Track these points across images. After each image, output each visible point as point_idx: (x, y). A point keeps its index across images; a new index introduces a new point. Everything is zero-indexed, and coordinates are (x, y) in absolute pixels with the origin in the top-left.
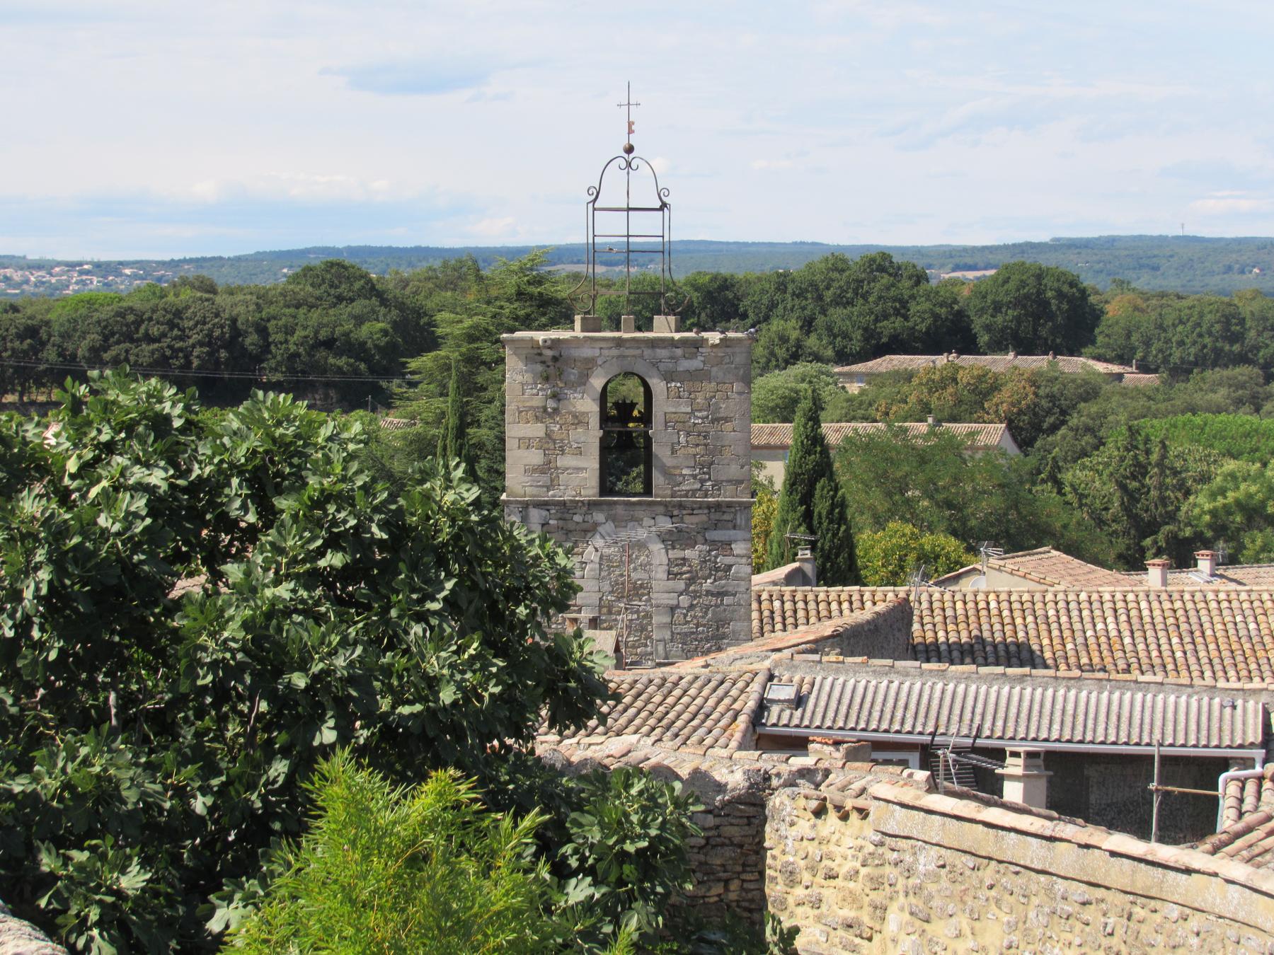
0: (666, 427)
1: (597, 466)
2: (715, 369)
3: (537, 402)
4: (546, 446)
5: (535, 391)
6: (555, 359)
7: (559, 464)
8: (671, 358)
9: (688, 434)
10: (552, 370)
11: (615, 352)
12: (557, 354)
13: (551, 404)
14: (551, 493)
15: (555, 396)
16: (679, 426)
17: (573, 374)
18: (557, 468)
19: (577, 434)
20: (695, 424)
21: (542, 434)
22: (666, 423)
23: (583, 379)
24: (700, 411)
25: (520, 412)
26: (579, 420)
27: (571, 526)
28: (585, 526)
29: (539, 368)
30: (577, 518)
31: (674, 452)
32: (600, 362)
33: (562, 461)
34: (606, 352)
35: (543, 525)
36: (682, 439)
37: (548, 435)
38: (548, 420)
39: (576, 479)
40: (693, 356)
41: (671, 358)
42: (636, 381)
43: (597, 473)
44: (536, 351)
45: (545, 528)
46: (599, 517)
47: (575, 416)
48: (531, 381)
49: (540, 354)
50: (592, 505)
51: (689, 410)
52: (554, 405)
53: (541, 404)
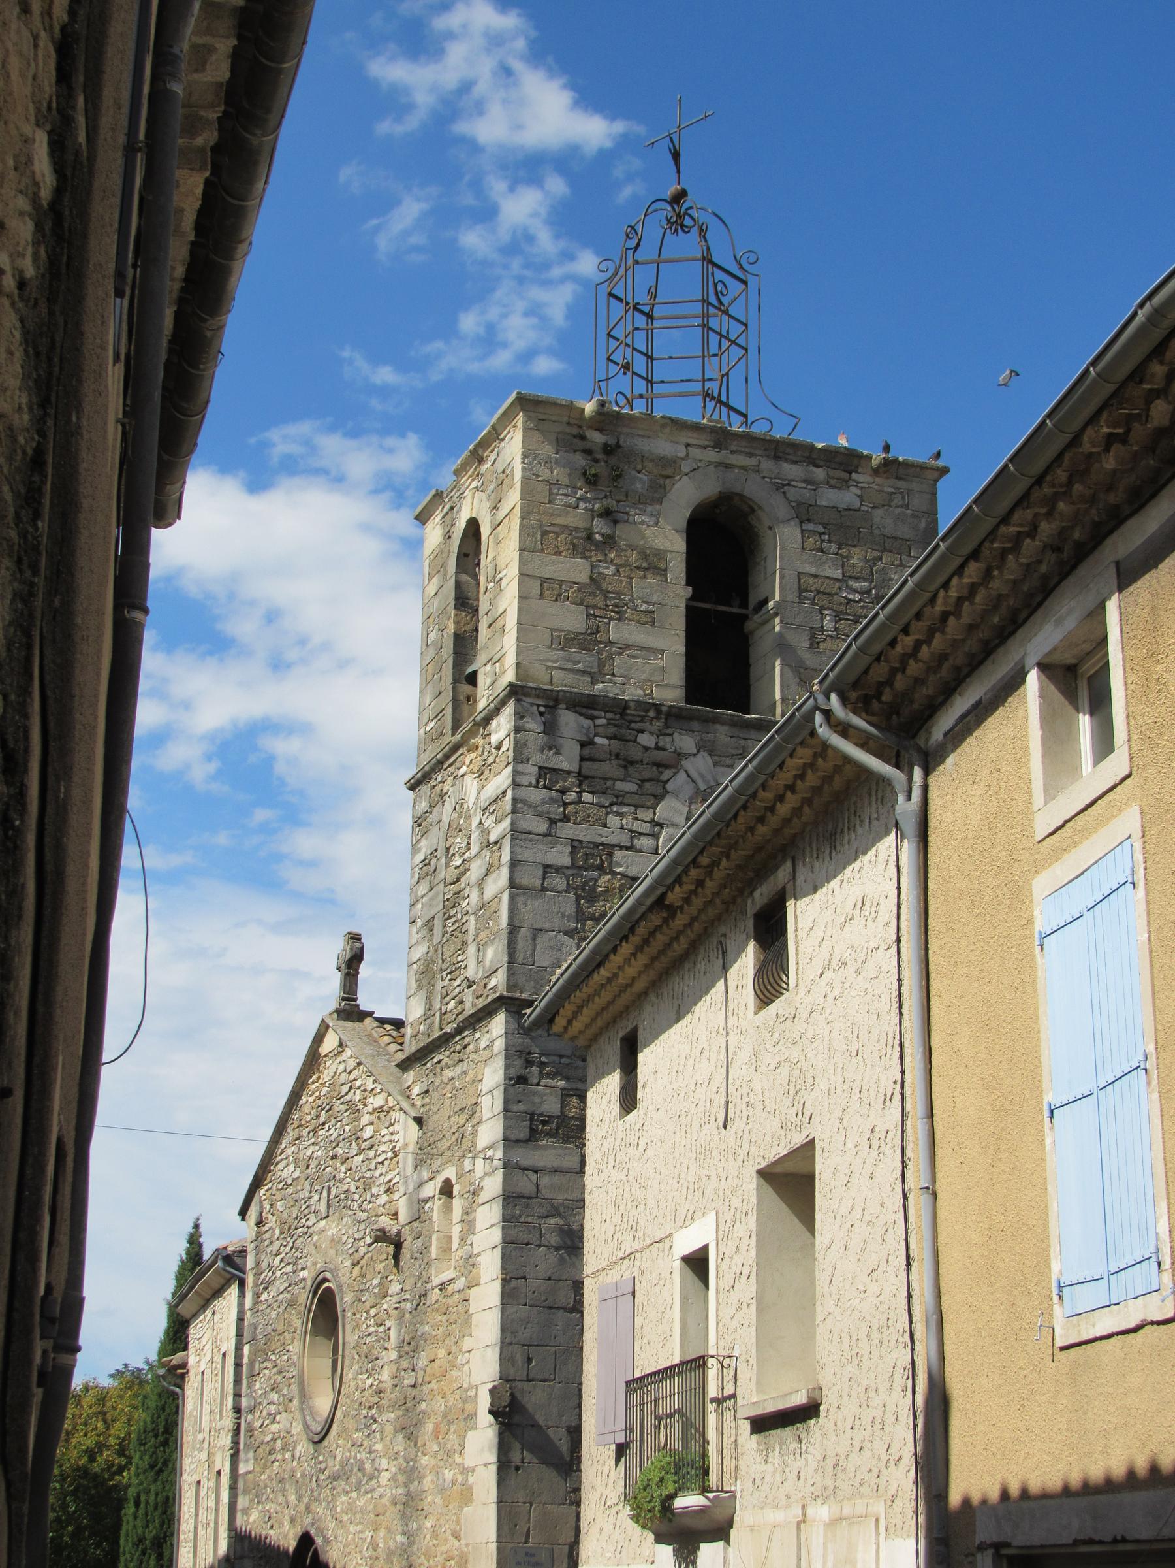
0: (802, 600)
1: (682, 649)
2: (878, 514)
3: (576, 519)
4: (590, 600)
5: (572, 500)
6: (608, 450)
7: (613, 637)
8: (806, 481)
9: (838, 617)
10: (600, 469)
11: (712, 455)
12: (612, 441)
13: (600, 527)
14: (598, 686)
15: (607, 513)
16: (822, 600)
17: (639, 482)
18: (610, 643)
19: (644, 587)
20: (849, 601)
21: (583, 577)
22: (801, 591)
23: (657, 492)
24: (857, 578)
25: (545, 533)
26: (652, 564)
27: (635, 753)
28: (659, 756)
29: (580, 460)
30: (646, 739)
31: (814, 644)
32: (686, 469)
33: (618, 632)
34: (695, 452)
35: (583, 745)
36: (828, 623)
37: (595, 581)
38: (596, 556)
39: (643, 668)
40: (843, 484)
41: (806, 481)
42: (695, 752)
43: (682, 662)
44: (575, 431)
45: (587, 751)
46: (685, 742)
47: (644, 555)
48: (564, 480)
49: (583, 438)
50: (672, 717)
51: (838, 574)
52: (606, 529)
53: (582, 524)
